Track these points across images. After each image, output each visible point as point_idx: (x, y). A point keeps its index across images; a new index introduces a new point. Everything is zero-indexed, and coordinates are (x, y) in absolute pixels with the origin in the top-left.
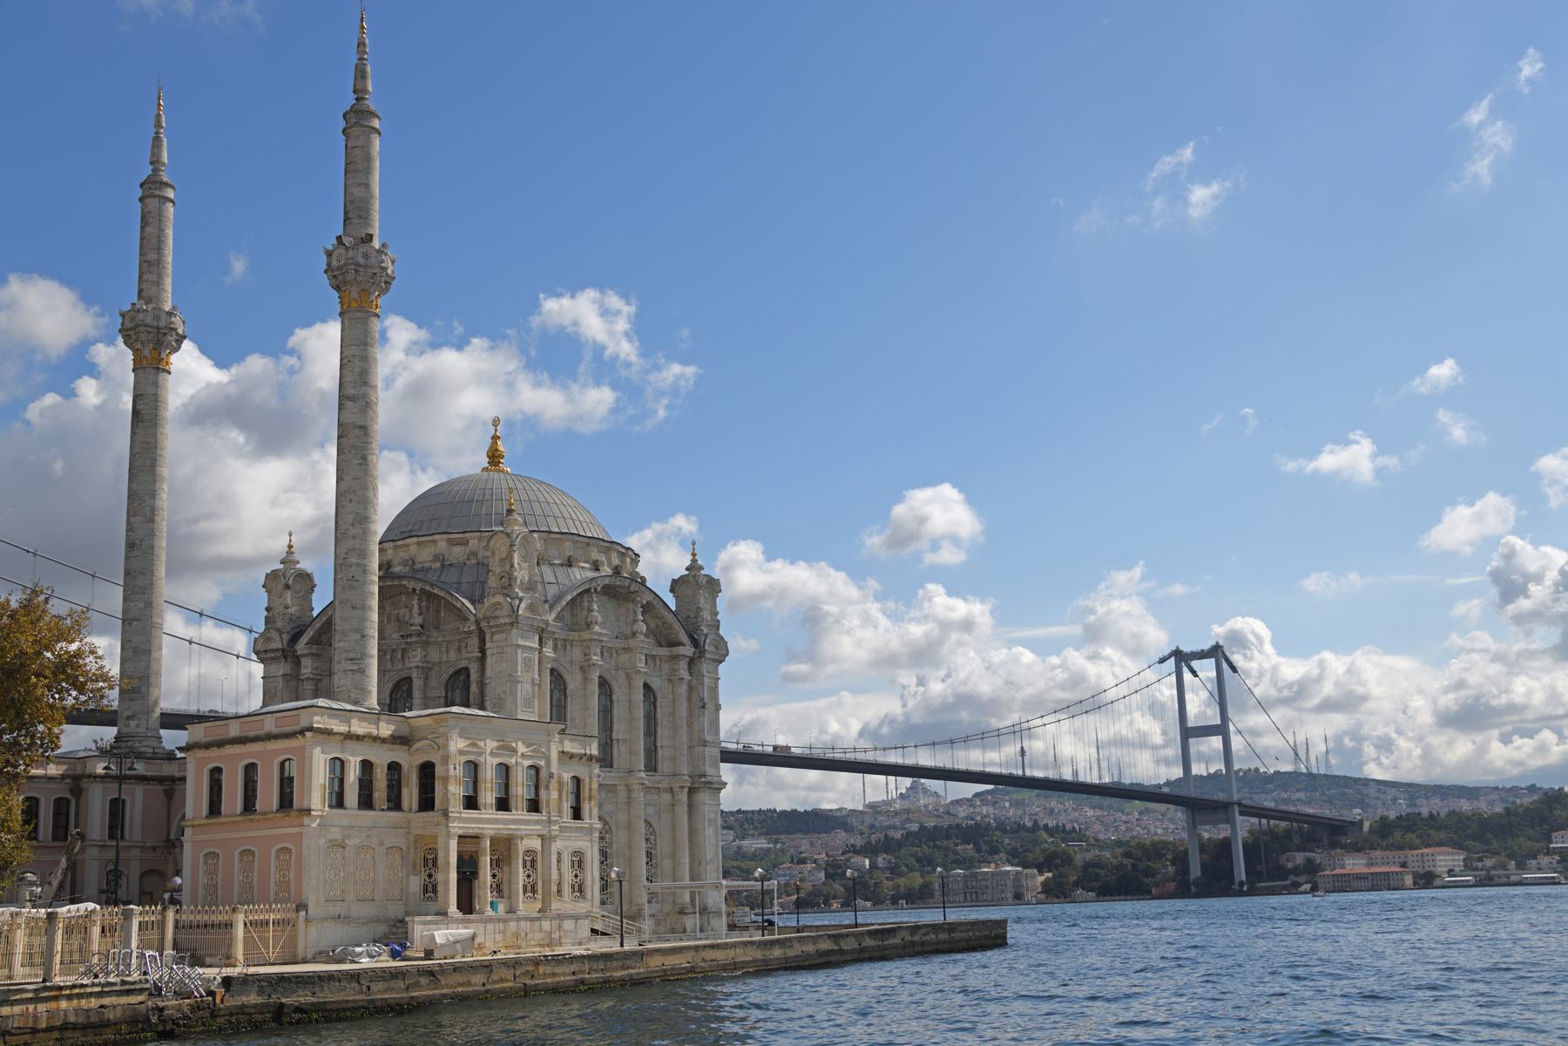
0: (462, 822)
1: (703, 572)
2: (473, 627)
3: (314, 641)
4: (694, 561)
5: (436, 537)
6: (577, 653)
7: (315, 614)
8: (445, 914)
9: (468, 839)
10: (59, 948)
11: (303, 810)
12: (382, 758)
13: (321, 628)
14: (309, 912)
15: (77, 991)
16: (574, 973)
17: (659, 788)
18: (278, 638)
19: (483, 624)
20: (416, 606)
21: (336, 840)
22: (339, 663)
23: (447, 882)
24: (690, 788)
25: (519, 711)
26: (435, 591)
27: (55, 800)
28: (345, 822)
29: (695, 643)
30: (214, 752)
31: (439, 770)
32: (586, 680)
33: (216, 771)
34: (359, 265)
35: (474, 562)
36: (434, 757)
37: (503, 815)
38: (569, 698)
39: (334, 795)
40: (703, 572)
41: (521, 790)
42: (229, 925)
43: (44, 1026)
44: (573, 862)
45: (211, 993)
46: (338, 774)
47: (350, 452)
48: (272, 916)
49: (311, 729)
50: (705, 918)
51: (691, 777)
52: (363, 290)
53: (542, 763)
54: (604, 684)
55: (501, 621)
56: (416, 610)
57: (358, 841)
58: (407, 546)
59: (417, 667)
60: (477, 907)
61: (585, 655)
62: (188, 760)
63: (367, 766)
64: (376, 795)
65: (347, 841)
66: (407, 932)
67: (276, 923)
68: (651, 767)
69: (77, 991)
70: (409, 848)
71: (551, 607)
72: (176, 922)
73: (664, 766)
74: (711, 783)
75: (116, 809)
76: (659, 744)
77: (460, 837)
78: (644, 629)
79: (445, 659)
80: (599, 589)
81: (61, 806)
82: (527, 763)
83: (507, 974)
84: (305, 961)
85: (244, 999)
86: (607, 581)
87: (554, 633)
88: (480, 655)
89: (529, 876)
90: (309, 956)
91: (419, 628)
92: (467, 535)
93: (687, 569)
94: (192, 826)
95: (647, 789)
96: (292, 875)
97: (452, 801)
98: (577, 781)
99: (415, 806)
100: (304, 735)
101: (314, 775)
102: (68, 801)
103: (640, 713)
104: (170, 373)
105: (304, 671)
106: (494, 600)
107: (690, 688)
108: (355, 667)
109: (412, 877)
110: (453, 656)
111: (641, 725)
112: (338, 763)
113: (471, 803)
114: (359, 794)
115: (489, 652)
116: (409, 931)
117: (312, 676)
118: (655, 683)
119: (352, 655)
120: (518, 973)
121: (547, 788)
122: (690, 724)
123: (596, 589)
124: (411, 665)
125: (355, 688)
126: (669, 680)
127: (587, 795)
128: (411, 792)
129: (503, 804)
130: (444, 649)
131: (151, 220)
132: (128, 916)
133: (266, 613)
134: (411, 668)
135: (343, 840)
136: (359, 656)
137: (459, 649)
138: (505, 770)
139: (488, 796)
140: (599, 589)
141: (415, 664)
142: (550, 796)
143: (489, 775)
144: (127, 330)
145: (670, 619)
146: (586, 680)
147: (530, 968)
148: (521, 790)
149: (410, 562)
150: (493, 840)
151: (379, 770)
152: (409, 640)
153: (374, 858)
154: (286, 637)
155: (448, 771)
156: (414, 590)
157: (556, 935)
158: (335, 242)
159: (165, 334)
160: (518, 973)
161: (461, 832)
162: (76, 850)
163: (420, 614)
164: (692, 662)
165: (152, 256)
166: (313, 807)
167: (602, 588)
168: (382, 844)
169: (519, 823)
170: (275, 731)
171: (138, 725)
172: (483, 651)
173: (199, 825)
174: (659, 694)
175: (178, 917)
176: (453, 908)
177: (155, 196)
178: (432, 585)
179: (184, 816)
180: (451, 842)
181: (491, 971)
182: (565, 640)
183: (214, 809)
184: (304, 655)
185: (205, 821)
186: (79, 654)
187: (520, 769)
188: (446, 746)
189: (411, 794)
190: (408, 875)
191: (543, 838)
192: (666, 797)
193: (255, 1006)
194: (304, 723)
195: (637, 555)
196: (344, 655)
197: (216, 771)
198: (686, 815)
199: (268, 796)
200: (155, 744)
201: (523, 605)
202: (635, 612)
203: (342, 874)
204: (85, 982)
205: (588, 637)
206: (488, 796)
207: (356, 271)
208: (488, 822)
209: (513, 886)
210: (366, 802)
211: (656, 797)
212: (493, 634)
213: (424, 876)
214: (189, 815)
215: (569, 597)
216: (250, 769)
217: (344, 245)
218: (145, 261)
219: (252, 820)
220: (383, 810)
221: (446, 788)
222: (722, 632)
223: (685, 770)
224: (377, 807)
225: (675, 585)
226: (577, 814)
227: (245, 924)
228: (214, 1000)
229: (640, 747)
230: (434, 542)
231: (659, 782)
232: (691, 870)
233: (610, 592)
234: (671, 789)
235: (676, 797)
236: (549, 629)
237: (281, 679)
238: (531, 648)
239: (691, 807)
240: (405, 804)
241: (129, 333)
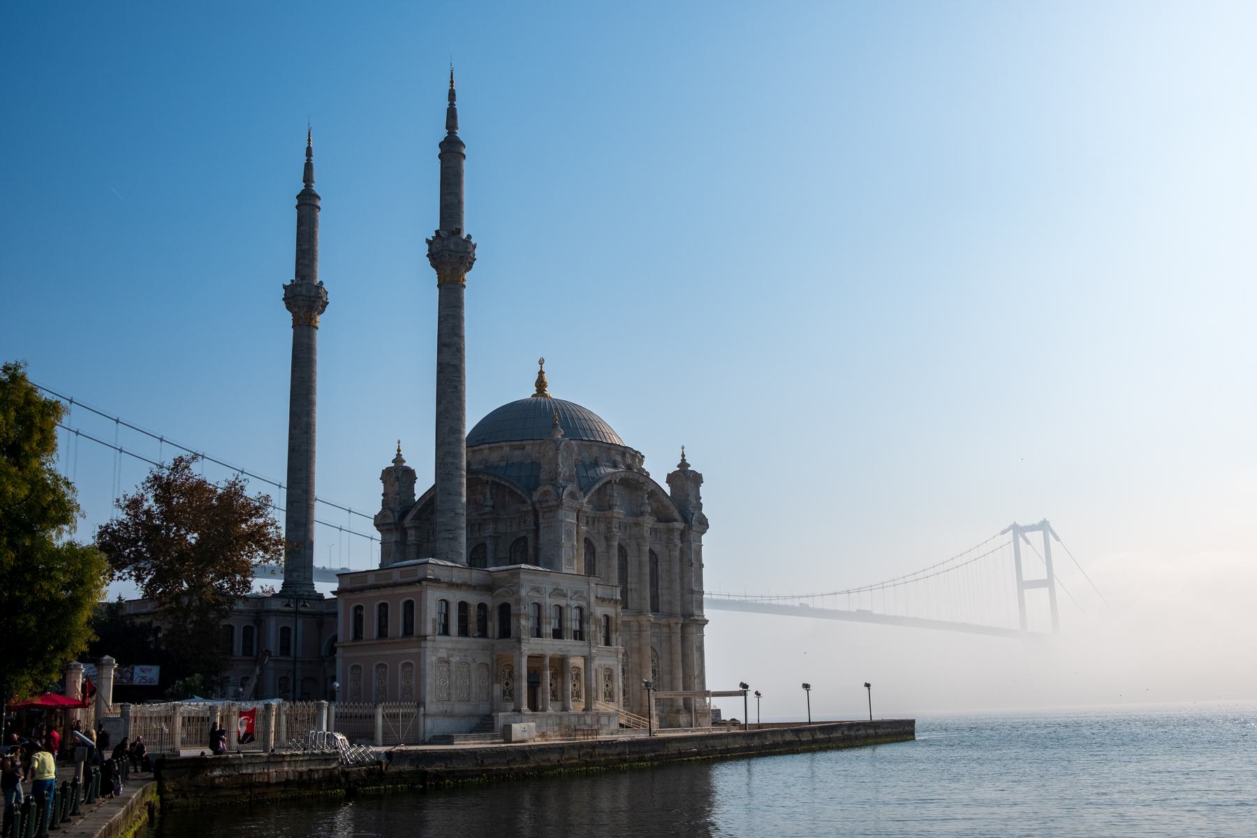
0: (531, 646)
1: (689, 469)
2: (530, 508)
3: (416, 517)
4: (683, 460)
5: (502, 444)
6: (602, 527)
7: (417, 498)
8: (520, 711)
9: (535, 659)
10: (273, 730)
11: (422, 637)
12: (473, 599)
13: (421, 508)
14: (427, 708)
15: (294, 759)
16: (619, 754)
17: (660, 624)
18: (391, 515)
19: (537, 506)
20: (488, 494)
21: (444, 658)
22: (440, 533)
23: (520, 689)
24: (682, 625)
25: (563, 568)
26: (502, 482)
27: (244, 627)
28: (449, 646)
29: (686, 520)
30: (357, 595)
31: (513, 609)
33: (359, 608)
34: (451, 251)
35: (529, 461)
36: (510, 600)
37: (557, 641)
38: (597, 559)
39: (441, 626)
40: (689, 469)
42: (372, 717)
43: (274, 781)
45: (379, 763)
46: (444, 611)
47: (446, 384)
48: (401, 711)
49: (426, 579)
52: (454, 269)
53: (583, 604)
54: (622, 550)
55: (550, 504)
56: (488, 495)
57: (458, 659)
58: (482, 450)
59: (490, 536)
60: (540, 707)
61: (608, 528)
62: (339, 600)
63: (463, 606)
64: (470, 626)
65: (451, 659)
66: (493, 724)
67: (404, 715)
68: (655, 609)
69: (294, 759)
70: (492, 663)
72: (336, 713)
73: (664, 608)
75: (285, 632)
77: (529, 657)
78: (650, 510)
79: (509, 530)
80: (617, 481)
81: (248, 631)
82: (574, 603)
83: (575, 754)
84: (425, 743)
85: (401, 768)
87: (586, 512)
88: (534, 527)
89: (607, 686)
90: (427, 740)
91: (491, 508)
92: (525, 442)
94: (343, 647)
95: (653, 625)
96: (413, 683)
97: (523, 631)
98: (607, 617)
99: (497, 635)
100: (421, 583)
101: (428, 611)
102: (252, 628)
103: (647, 570)
104: (317, 328)
105: (409, 539)
106: (545, 489)
107: (682, 552)
108: (451, 536)
109: (495, 685)
111: (648, 578)
112: (444, 603)
114: (459, 626)
115: (542, 526)
116: (495, 722)
117: (415, 542)
118: (657, 548)
119: (449, 528)
120: (581, 753)
121: (588, 623)
122: (682, 578)
123: (615, 481)
124: (485, 535)
125: (452, 551)
127: (614, 628)
128: (494, 625)
130: (509, 524)
131: (304, 221)
132: (320, 708)
134: (485, 537)
135: (448, 657)
136: (453, 528)
139: (548, 629)
140: (617, 481)
141: (489, 534)
142: (591, 628)
144: (288, 299)
145: (667, 502)
146: (609, 547)
147: (590, 750)
149: (484, 462)
150: (551, 659)
151: (472, 609)
152: (484, 517)
153: (469, 671)
154: (397, 515)
155: (520, 610)
156: (487, 481)
158: (434, 235)
159: (314, 301)
160: (581, 753)
161: (530, 653)
162: (265, 662)
163: (492, 499)
164: (683, 535)
165: (306, 247)
166: (428, 634)
168: (474, 661)
169: (567, 645)
170: (400, 580)
171: (298, 576)
172: (537, 524)
173: (347, 646)
174: (659, 557)
175: (337, 710)
176: (525, 708)
178: (500, 478)
179: (335, 639)
180: (523, 659)
181: (563, 752)
182: (594, 518)
183: (358, 634)
184: (409, 528)
185: (378, 642)
186: (265, 525)
187: (569, 609)
188: (518, 592)
189: (493, 626)
190: (493, 683)
192: (665, 630)
193: (408, 772)
194: (420, 575)
195: (643, 456)
196: (443, 528)
198: (680, 644)
200: (310, 589)
201: (565, 492)
202: (642, 497)
203: (448, 682)
204: (299, 753)
206: (548, 629)
207: (449, 255)
208: (548, 646)
209: (565, 692)
210: (463, 631)
211: (658, 630)
212: (544, 513)
213: (503, 684)
214: (340, 639)
215: (597, 486)
216: (383, 608)
217: (441, 237)
218: (301, 250)
219: (385, 643)
220: (475, 637)
221: (519, 622)
222: (704, 511)
223: (678, 609)
224: (471, 635)
225: (671, 479)
226: (608, 643)
227: (383, 716)
228: (381, 767)
229: (647, 594)
230: (501, 447)
232: (684, 682)
233: (625, 483)
234: (669, 624)
235: (673, 631)
236: (583, 509)
237: (393, 545)
239: (684, 639)
240: (490, 633)
241: (290, 300)
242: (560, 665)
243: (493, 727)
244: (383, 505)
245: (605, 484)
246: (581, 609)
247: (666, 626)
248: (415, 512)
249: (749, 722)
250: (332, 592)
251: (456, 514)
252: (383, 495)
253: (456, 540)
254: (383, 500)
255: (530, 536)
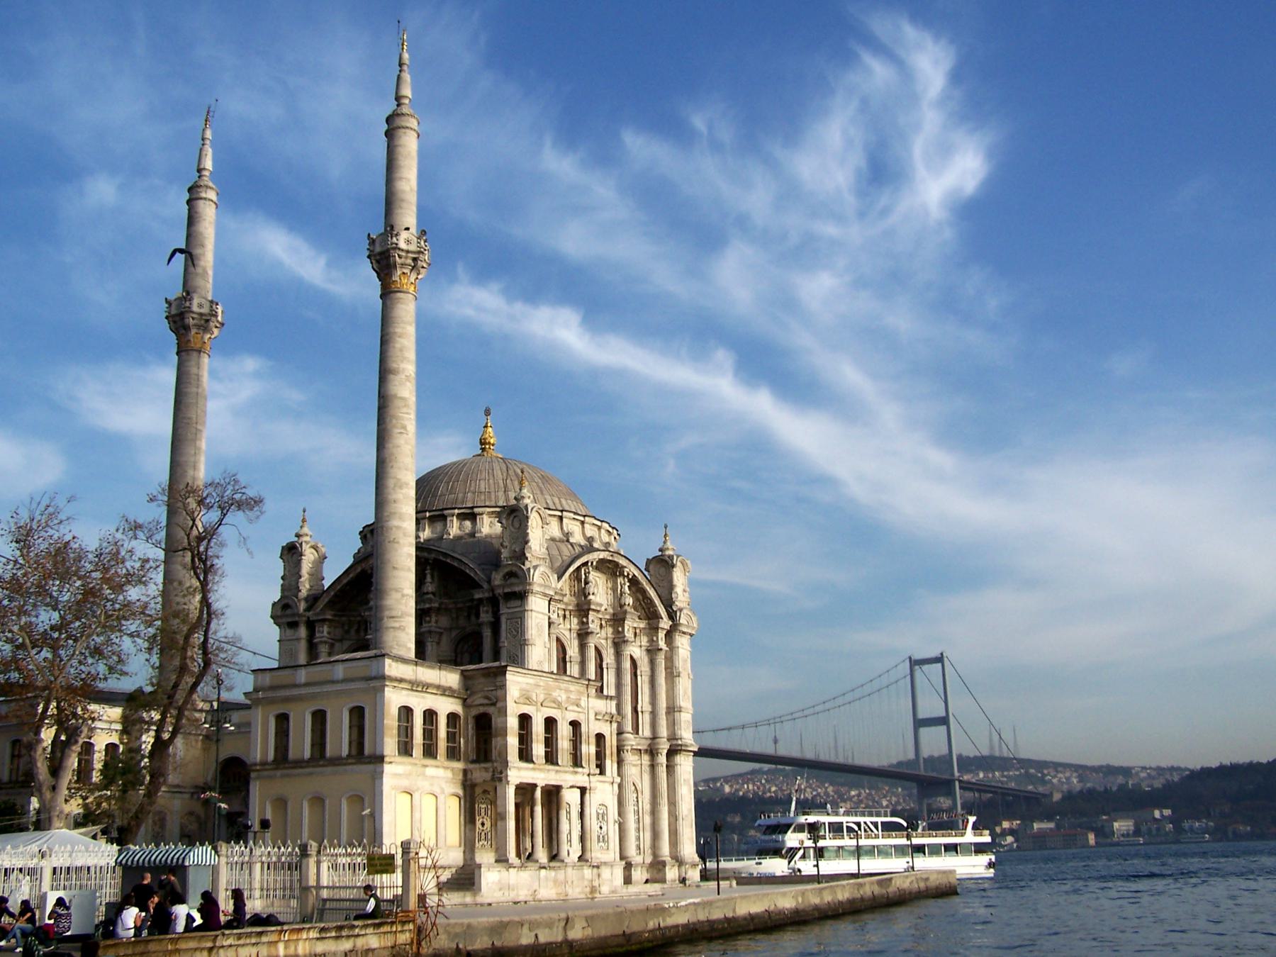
0: (518, 773)
5: (446, 512)
7: (327, 584)
8: (507, 861)
9: (525, 791)
12: (446, 706)
24: (669, 751)
26: (448, 561)
29: (672, 616)
31: (496, 721)
32: (583, 647)
36: (491, 710)
41: (564, 744)
44: (598, 814)
50: (683, 869)
51: (668, 740)
52: (404, 273)
53: (581, 718)
59: (430, 632)
61: (583, 623)
63: (430, 715)
71: (559, 578)
74: (686, 746)
76: (639, 709)
80: (594, 563)
82: (572, 716)
86: (601, 557)
88: (492, 620)
93: (661, 550)
103: (627, 678)
110: (462, 622)
113: (525, 755)
119: (394, 613)
123: (592, 563)
126: (648, 651)
129: (551, 758)
130: (454, 616)
133: (281, 582)
137: (469, 617)
138: (550, 723)
139: (539, 749)
140: (594, 563)
142: (589, 749)
143: (538, 728)
148: (564, 744)
157: (596, 884)
164: (669, 635)
167: (597, 562)
177: (201, 199)
182: (564, 610)
191: (583, 790)
197: (283, 719)
198: (665, 775)
199: (339, 740)
205: (586, 607)
206: (539, 749)
208: (541, 776)
210: (430, 751)
216: (319, 718)
231: (638, 744)
238: (543, 613)
242: (553, 794)
243: (473, 884)
244: (283, 590)
245: (578, 569)
246: (575, 725)
247: (646, 751)
248: (326, 600)
249: (821, 873)
250: (245, 694)
251: (403, 596)
252: (282, 578)
253: (404, 630)
254: (282, 585)
255: (487, 633)
